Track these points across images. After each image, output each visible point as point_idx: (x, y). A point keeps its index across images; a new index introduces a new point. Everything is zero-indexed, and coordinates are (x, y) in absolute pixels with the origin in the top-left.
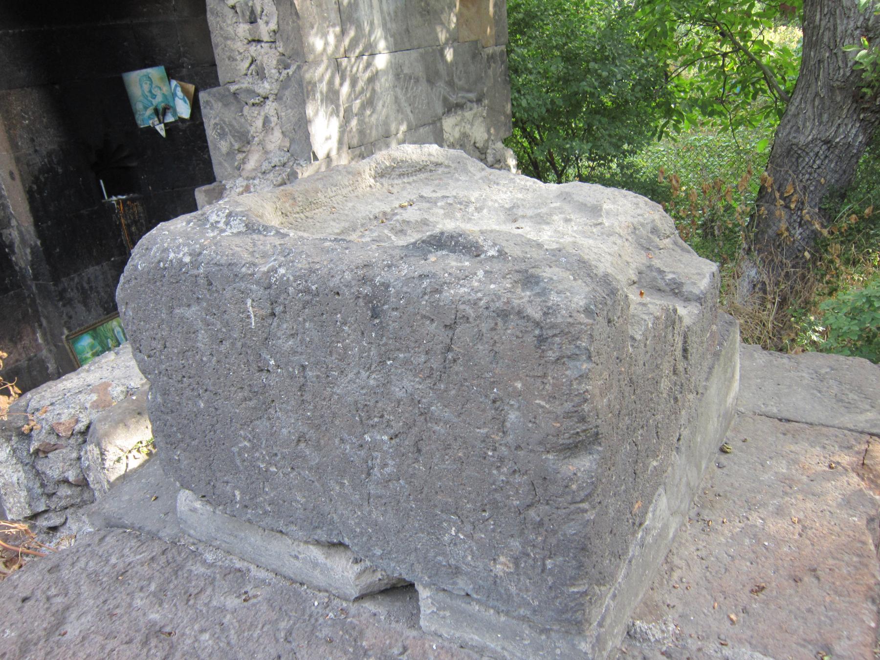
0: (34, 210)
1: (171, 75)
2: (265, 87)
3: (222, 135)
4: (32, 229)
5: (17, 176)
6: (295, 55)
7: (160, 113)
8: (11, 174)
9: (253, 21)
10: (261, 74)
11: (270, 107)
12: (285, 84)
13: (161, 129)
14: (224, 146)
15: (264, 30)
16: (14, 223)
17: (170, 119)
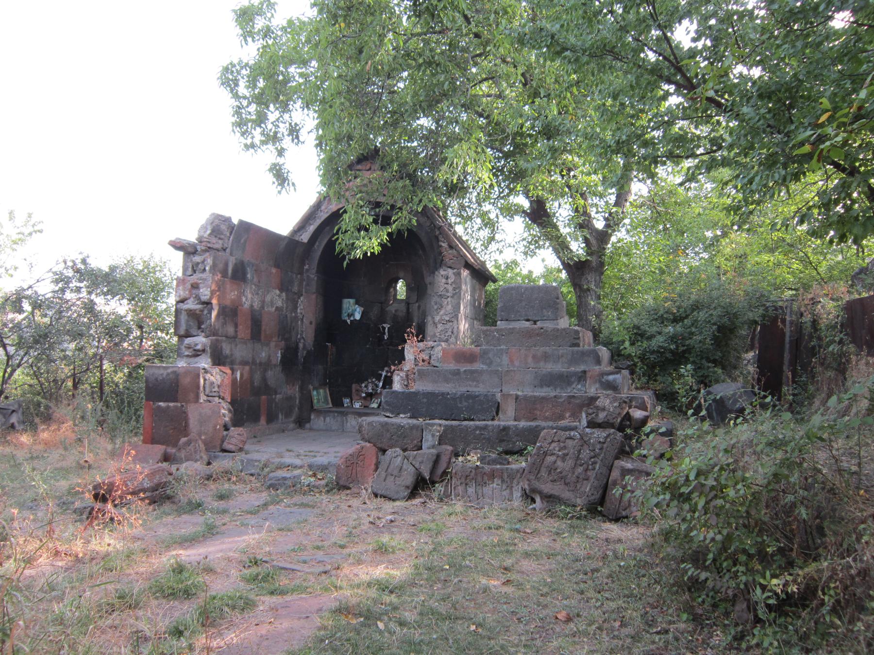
0: (315, 337)
1: (357, 303)
2: (449, 294)
3: (436, 304)
4: (312, 343)
5: (314, 323)
6: (457, 288)
7: (349, 316)
8: (311, 323)
9: (447, 279)
10: (447, 291)
11: (449, 299)
12: (454, 294)
13: (349, 321)
14: (436, 307)
15: (450, 281)
16: (302, 341)
17: (352, 318)
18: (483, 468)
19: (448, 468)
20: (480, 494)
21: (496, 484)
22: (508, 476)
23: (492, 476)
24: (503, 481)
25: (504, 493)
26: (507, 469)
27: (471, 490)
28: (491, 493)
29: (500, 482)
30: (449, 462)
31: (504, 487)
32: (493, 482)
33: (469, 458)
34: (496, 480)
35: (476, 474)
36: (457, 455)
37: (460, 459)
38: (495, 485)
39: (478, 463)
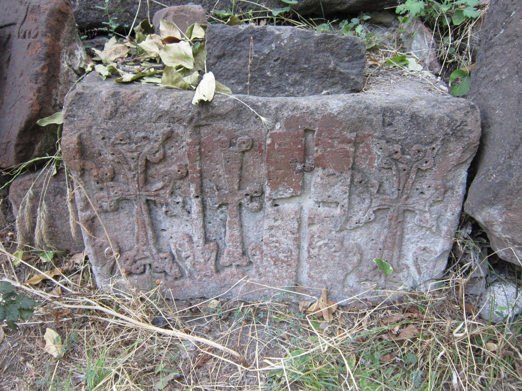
18: (238, 112)
19: (47, 104)
20: (230, 247)
21: (315, 200)
22: (393, 159)
23: (296, 156)
24: (359, 184)
25: (359, 238)
26: (388, 115)
27: (180, 229)
28: (287, 242)
29: (339, 191)
30: (51, 76)
31: (360, 215)
32: (301, 189)
33: (149, 45)
34: (316, 178)
35: (201, 151)
36: (93, 32)
37: (112, 49)
38: (308, 203)
39: (207, 88)
